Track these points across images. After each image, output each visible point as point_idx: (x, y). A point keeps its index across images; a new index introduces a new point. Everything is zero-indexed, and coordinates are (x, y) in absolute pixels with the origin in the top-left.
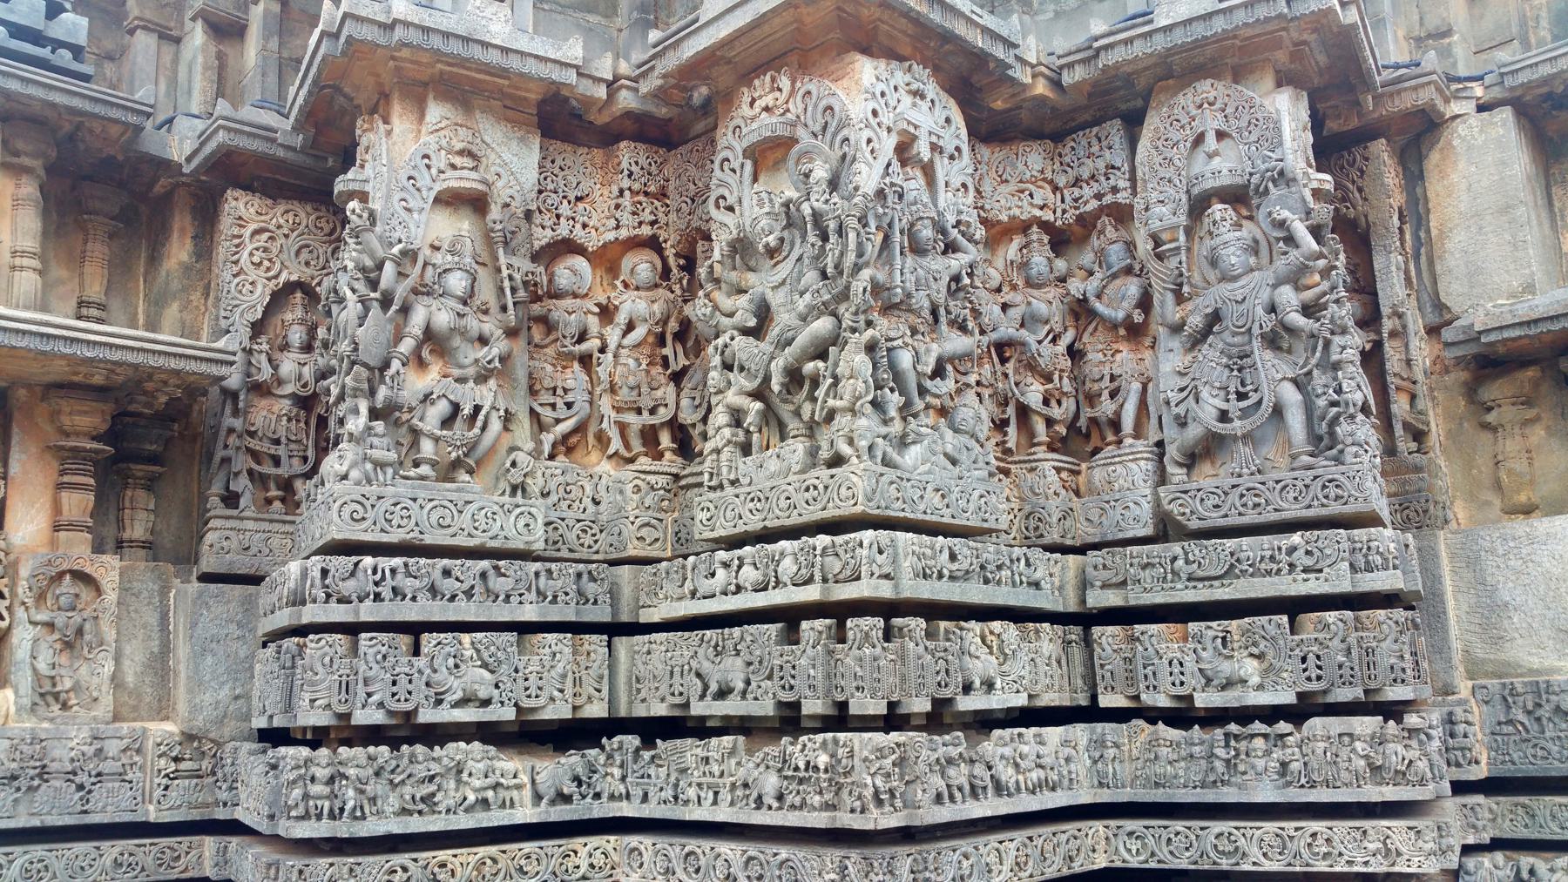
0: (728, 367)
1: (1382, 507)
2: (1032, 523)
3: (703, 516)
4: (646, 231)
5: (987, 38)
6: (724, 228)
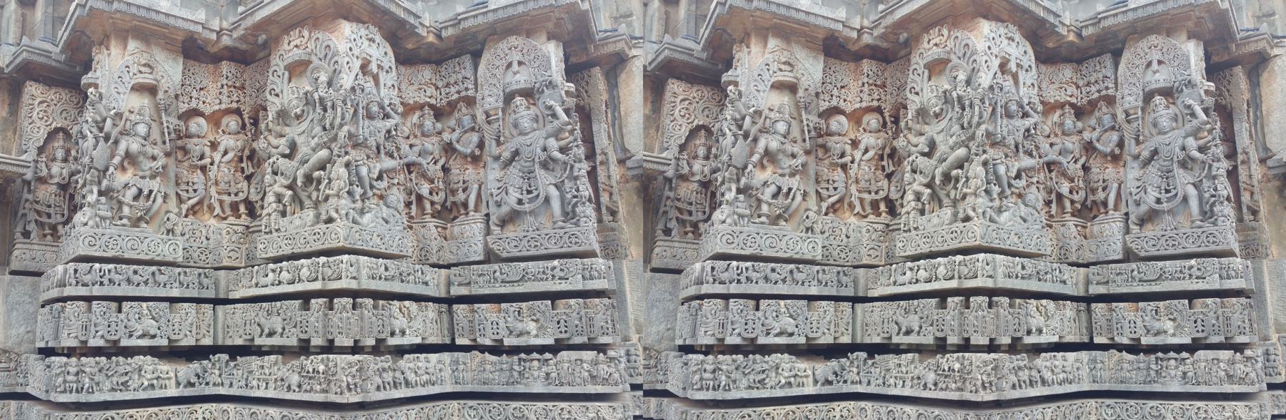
0: (914, 171)
1: (1236, 247)
2: (1063, 252)
3: (900, 245)
4: (875, 103)
5: (1045, 12)
6: (914, 103)
